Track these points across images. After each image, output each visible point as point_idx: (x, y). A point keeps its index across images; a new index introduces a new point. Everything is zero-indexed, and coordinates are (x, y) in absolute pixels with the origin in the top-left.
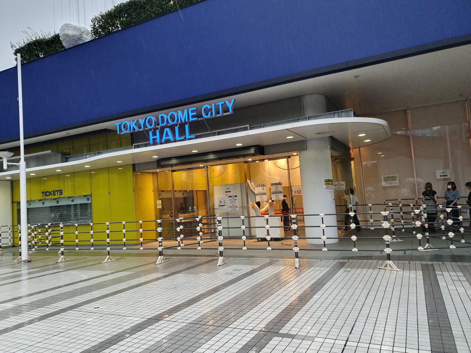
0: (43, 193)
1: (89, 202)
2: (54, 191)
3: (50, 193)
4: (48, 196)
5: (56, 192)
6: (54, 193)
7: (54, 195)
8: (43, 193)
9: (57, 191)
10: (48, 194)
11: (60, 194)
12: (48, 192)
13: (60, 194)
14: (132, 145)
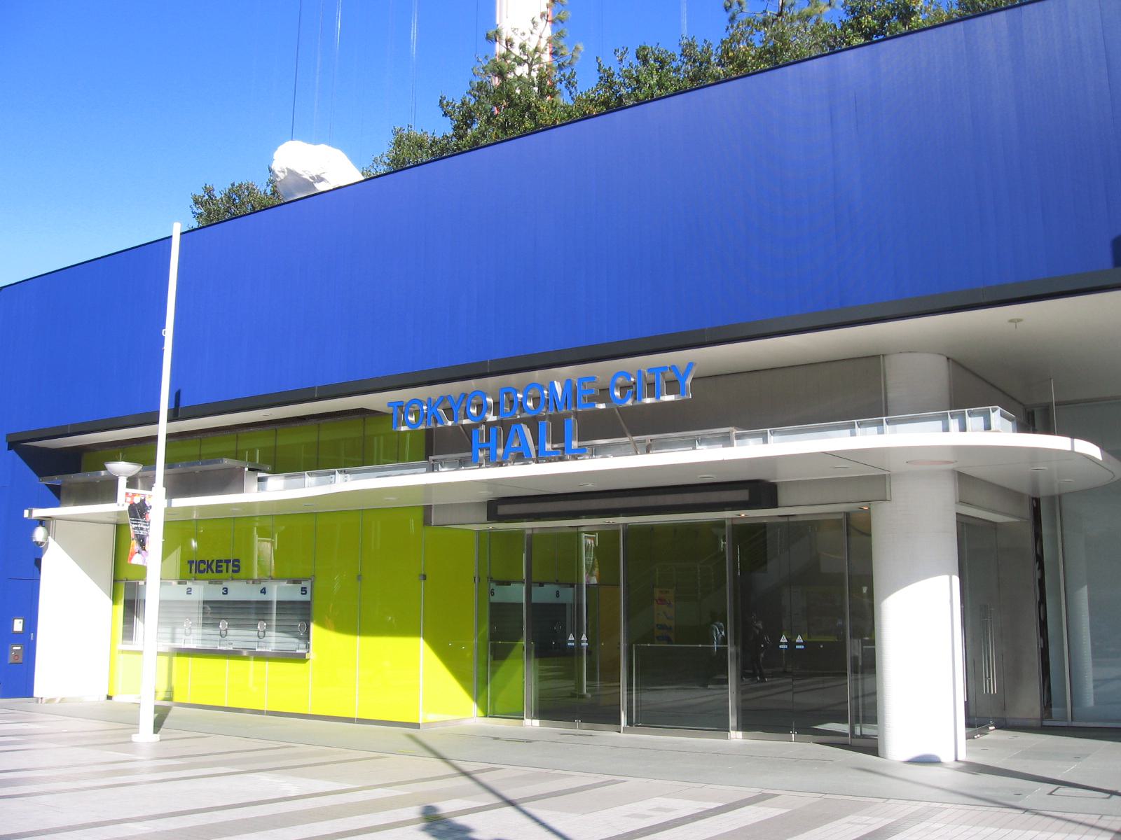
0: (191, 562)
1: (307, 598)
2: (218, 561)
3: (209, 566)
4: (202, 572)
5: (224, 565)
6: (217, 566)
7: (218, 571)
8: (191, 562)
9: (228, 561)
10: (203, 567)
11: (234, 571)
12: (202, 561)
13: (234, 571)
14: (427, 459)
